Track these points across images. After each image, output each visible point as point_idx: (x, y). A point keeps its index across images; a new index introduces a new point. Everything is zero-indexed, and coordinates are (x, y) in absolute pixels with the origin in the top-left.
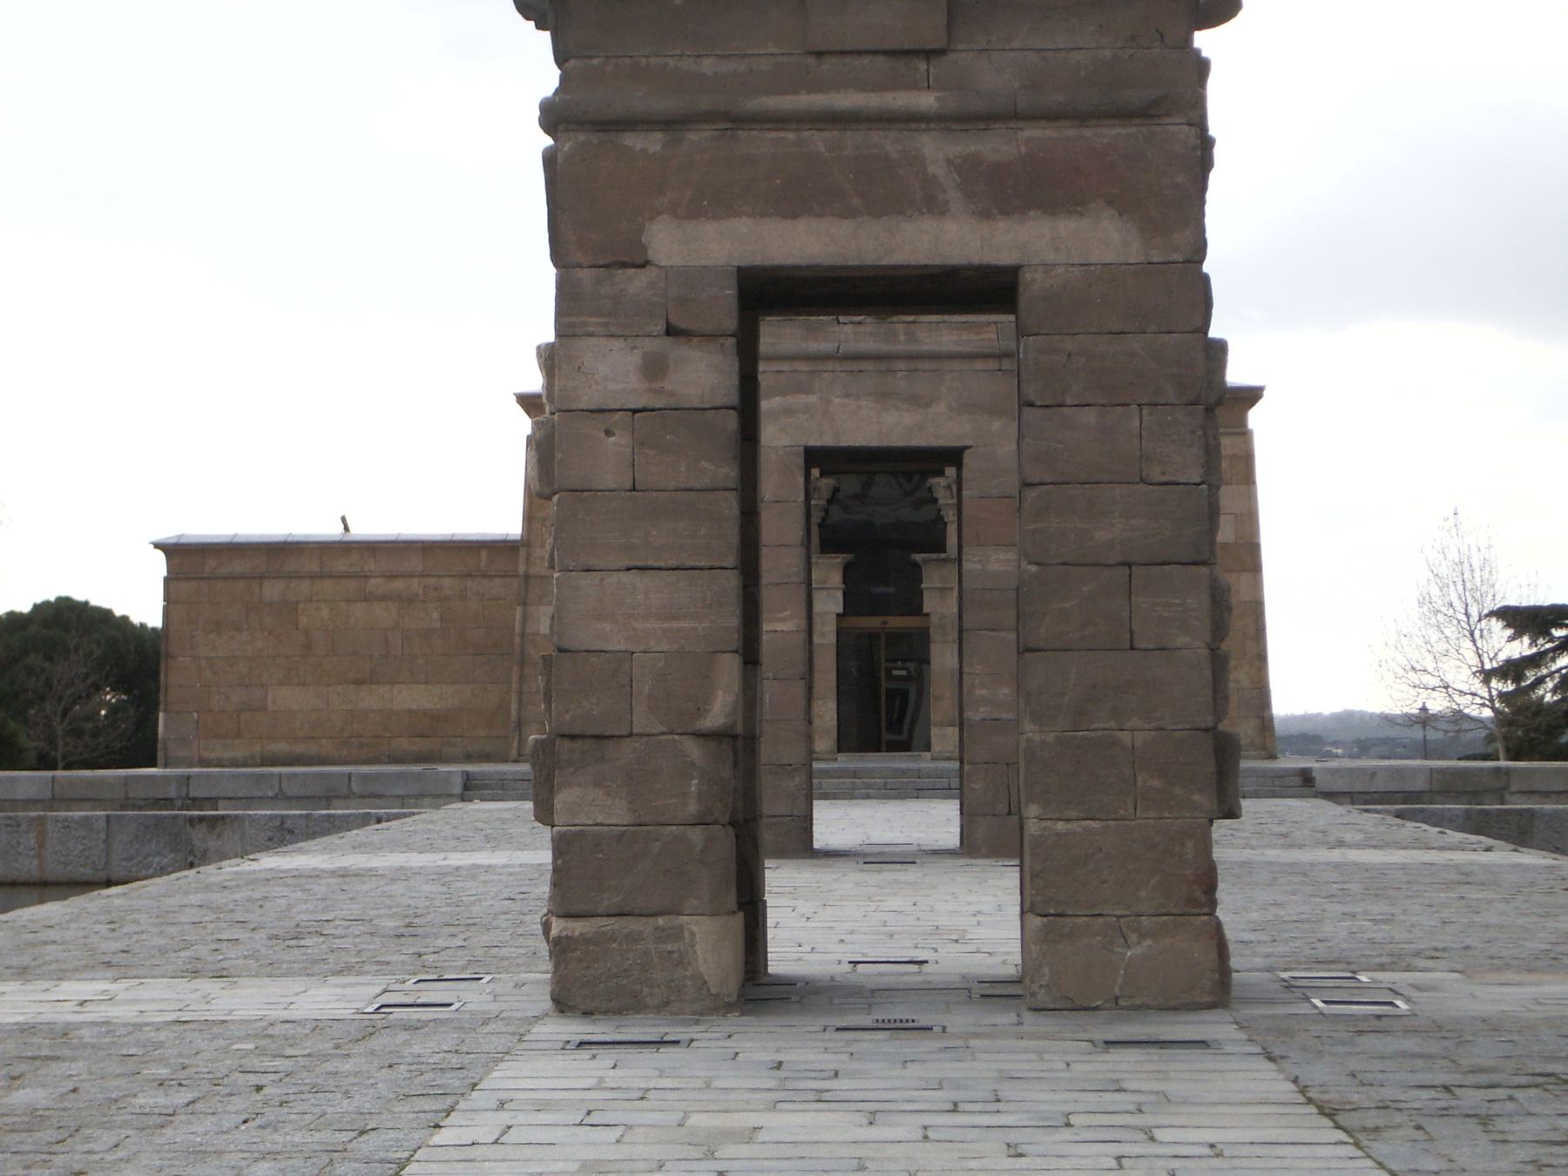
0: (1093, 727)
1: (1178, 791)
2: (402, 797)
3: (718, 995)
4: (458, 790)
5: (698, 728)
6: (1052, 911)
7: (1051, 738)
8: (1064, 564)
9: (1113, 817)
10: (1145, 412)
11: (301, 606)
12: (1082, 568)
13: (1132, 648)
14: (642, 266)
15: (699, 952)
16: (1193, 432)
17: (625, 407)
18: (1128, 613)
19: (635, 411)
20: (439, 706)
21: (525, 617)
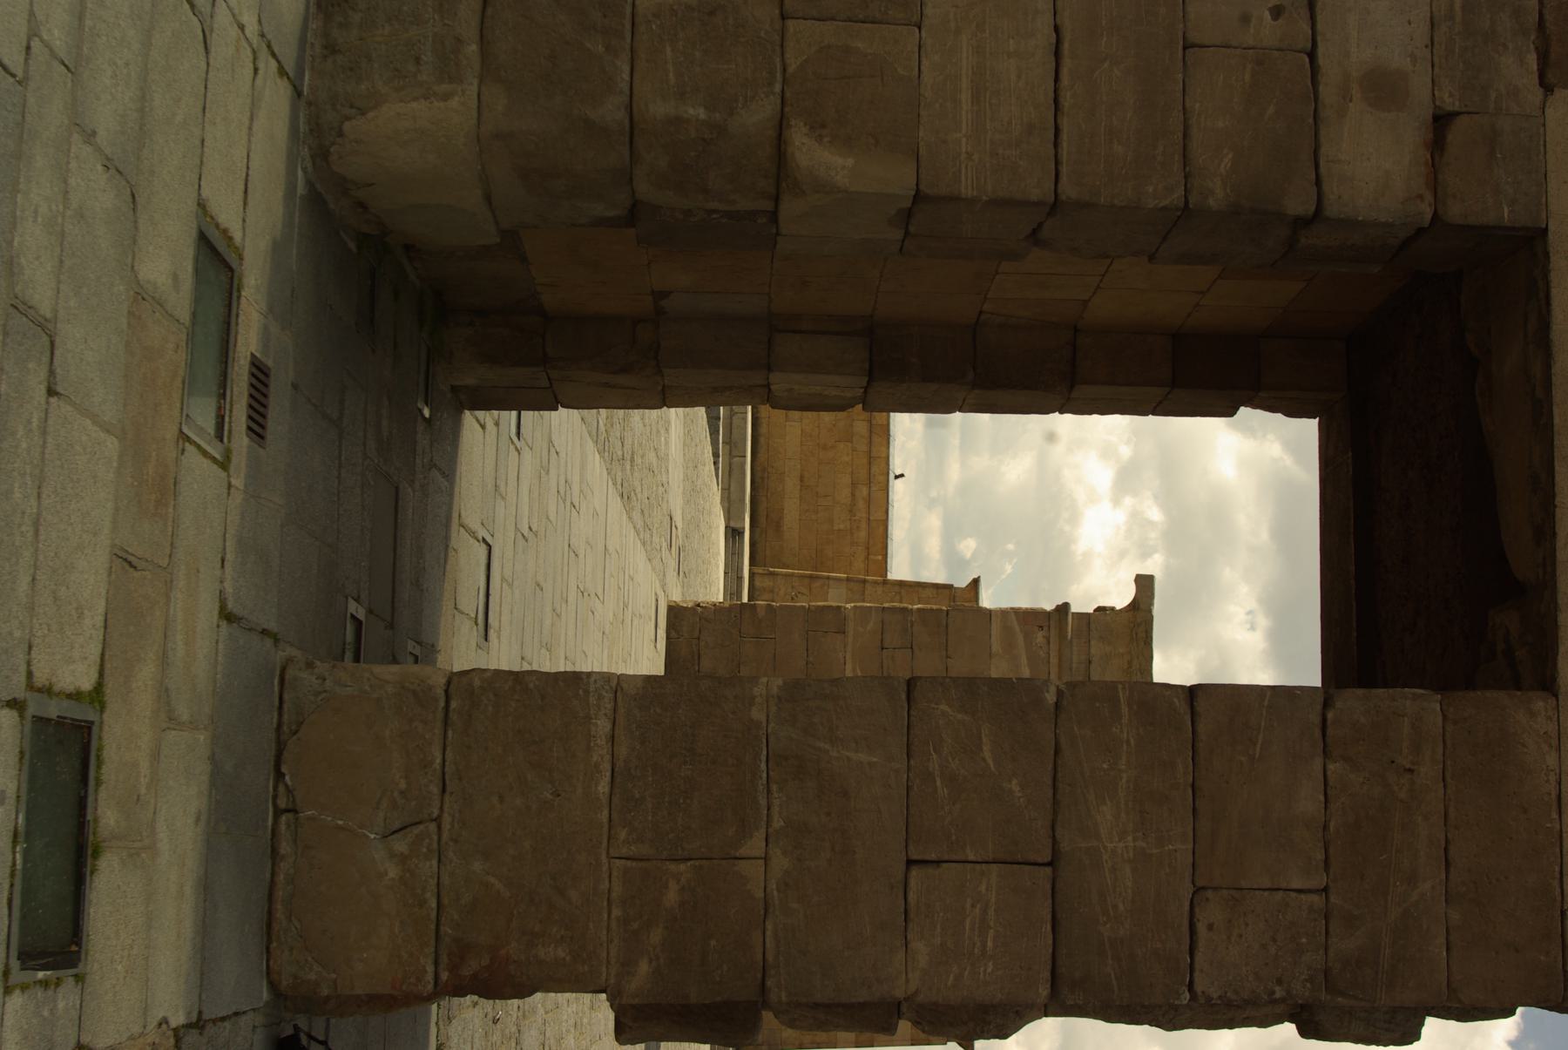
0: (774, 787)
1: (656, 936)
2: (729, 489)
3: (341, 134)
4: (732, 524)
5: (793, 123)
6: (454, 704)
7: (757, 714)
8: (1057, 751)
9: (615, 816)
10: (1315, 898)
11: (850, 445)
12: (1048, 780)
13: (910, 863)
14: (1542, 82)
15: (414, 105)
16: (1279, 982)
17: (1319, 38)
18: (971, 858)
19: (1312, 55)
20: (785, 527)
21: (838, 580)
